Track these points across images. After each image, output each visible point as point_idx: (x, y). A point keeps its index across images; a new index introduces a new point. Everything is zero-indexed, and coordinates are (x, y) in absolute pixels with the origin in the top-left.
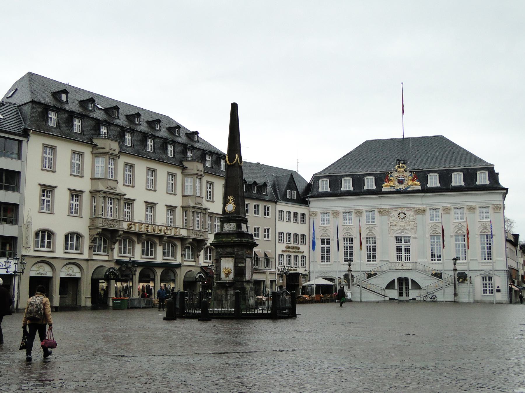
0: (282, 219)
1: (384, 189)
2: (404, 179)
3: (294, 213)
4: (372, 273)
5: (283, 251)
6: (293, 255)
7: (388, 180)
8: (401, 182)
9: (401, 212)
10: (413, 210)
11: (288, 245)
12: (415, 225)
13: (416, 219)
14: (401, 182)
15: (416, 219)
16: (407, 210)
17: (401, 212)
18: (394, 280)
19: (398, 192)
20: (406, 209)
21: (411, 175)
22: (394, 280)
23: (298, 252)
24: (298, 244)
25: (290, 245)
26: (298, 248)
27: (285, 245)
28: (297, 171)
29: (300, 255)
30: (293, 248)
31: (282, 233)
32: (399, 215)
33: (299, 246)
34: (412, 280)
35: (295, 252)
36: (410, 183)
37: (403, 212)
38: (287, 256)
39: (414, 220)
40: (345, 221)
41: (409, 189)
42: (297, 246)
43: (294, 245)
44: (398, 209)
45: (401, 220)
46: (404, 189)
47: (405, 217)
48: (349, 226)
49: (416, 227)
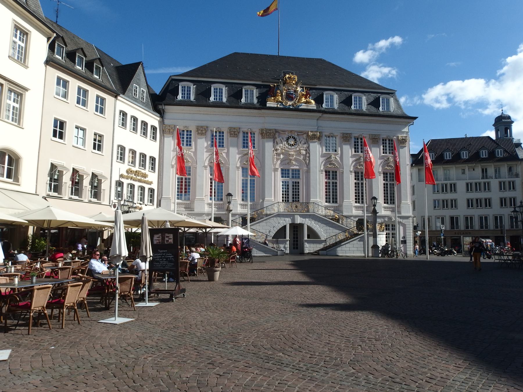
0: (124, 124)
1: (270, 104)
5: (121, 176)
6: (137, 184)
9: (290, 137)
14: (289, 97)
17: (290, 137)
18: (285, 227)
19: (285, 109)
22: (285, 227)
23: (145, 182)
25: (134, 169)
26: (145, 176)
29: (147, 187)
30: (137, 173)
32: (293, 137)
34: (308, 227)
35: (140, 181)
37: (293, 137)
38: (128, 184)
41: (300, 108)
42: (143, 171)
43: (140, 170)
45: (290, 147)
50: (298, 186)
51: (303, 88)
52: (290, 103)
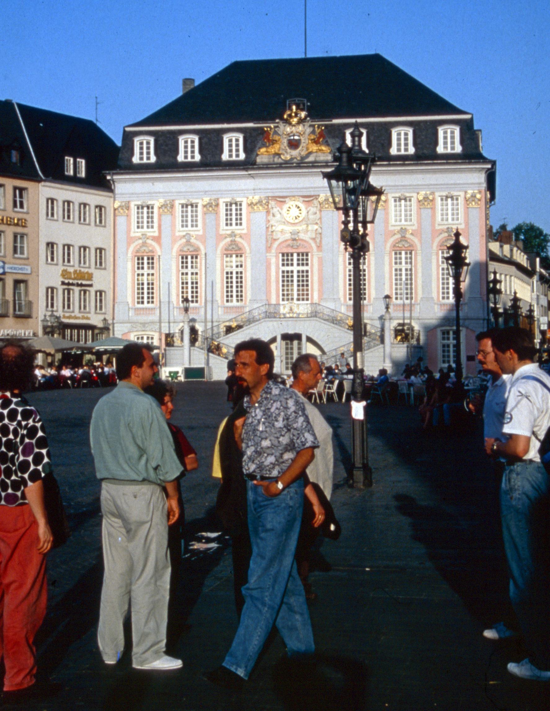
2: (300, 140)
3: (80, 204)
4: (234, 324)
7: (269, 140)
8: (294, 144)
10: (315, 202)
11: (65, 268)
12: (320, 230)
13: (320, 218)
14: (294, 144)
15: (320, 218)
16: (304, 201)
20: (302, 199)
21: (313, 132)
24: (89, 267)
27: (61, 268)
28: (95, 121)
31: (51, 245)
32: (288, 210)
33: (92, 270)
36: (314, 148)
39: (317, 221)
40: (184, 224)
44: (287, 200)
46: (299, 158)
47: (299, 215)
48: (191, 233)
49: (320, 234)
50: (307, 276)
51: (313, 126)
52: (295, 153)
